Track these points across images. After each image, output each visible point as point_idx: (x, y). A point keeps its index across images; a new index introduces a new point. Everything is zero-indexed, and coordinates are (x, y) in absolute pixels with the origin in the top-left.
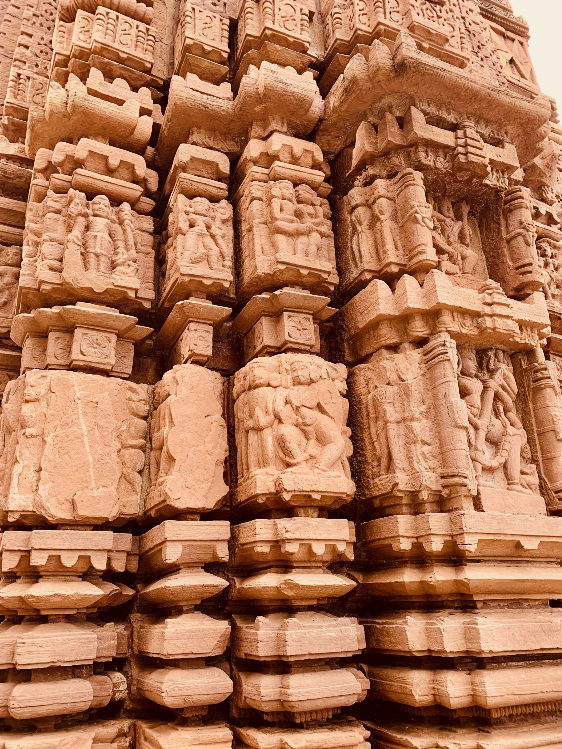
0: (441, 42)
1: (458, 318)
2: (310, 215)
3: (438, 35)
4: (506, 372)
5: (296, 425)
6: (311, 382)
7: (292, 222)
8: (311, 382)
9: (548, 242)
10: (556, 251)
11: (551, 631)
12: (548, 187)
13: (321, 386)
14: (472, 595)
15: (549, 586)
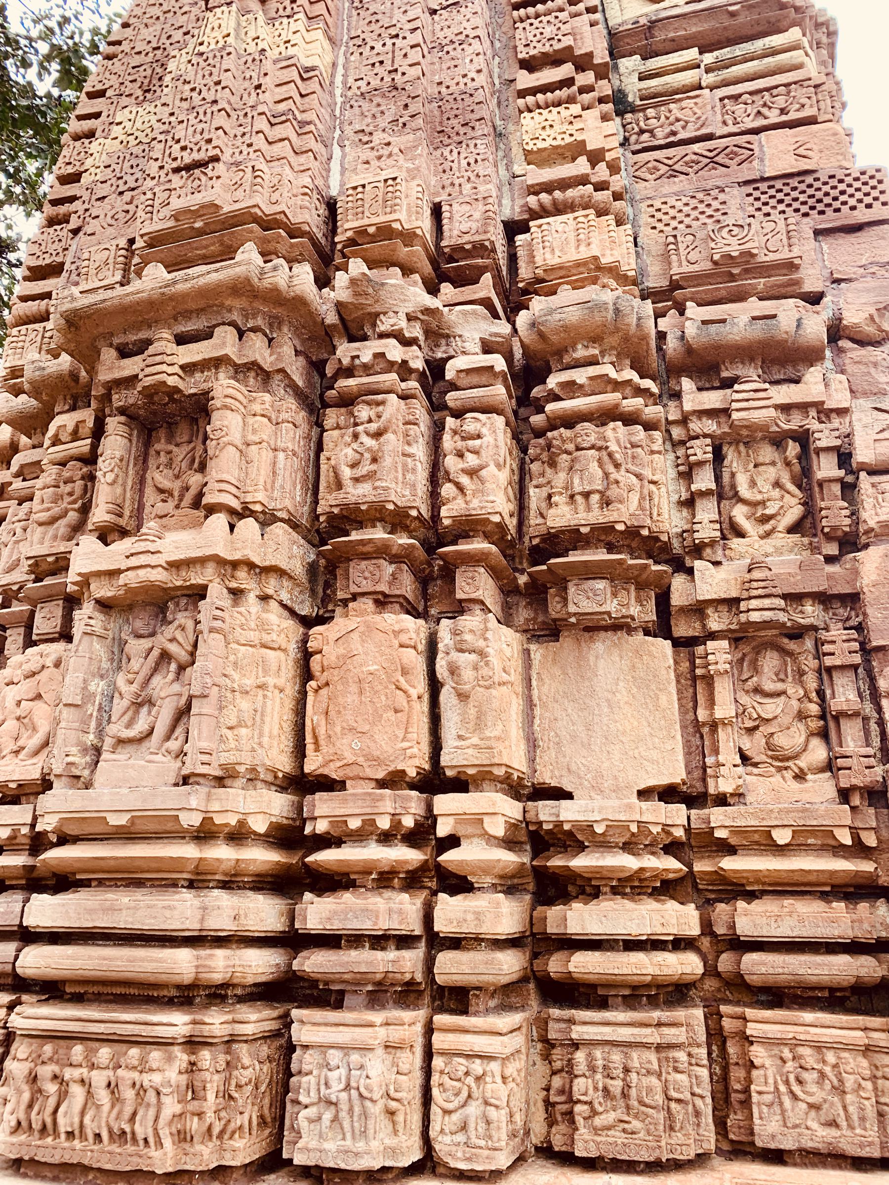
0: (212, 210)
1: (105, 581)
2: (71, 494)
3: (203, 206)
4: (183, 621)
5: (18, 719)
6: (34, 674)
7: (49, 509)
8: (34, 674)
9: (364, 402)
10: (381, 408)
11: (113, 909)
12: (385, 313)
13: (43, 676)
14: (74, 874)
15: (154, 865)
